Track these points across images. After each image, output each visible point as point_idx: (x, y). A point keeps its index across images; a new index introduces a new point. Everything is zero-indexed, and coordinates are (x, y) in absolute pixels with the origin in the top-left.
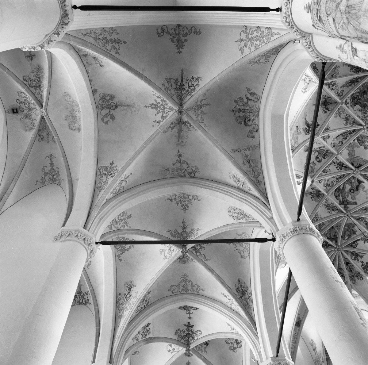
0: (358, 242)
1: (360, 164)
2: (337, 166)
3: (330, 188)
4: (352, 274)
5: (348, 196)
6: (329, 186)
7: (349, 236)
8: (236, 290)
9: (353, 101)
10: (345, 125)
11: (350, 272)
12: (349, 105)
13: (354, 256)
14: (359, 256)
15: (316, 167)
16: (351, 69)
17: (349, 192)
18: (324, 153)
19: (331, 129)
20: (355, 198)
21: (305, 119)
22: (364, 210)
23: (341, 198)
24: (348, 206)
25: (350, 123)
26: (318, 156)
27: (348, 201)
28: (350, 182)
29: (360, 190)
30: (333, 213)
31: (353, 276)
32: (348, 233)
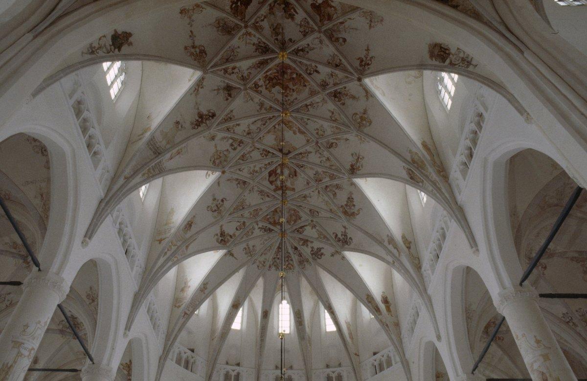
0: (306, 228)
1: (289, 151)
2: (261, 152)
3: (257, 174)
5: (287, 180)
6: (257, 172)
7: (295, 221)
8: (87, 297)
9: (269, 83)
10: (258, 111)
12: (263, 89)
13: (303, 241)
15: (230, 155)
16: (256, 49)
19: (236, 117)
21: (198, 109)
23: (279, 183)
24: (286, 192)
25: (266, 109)
30: (267, 199)
32: (294, 218)
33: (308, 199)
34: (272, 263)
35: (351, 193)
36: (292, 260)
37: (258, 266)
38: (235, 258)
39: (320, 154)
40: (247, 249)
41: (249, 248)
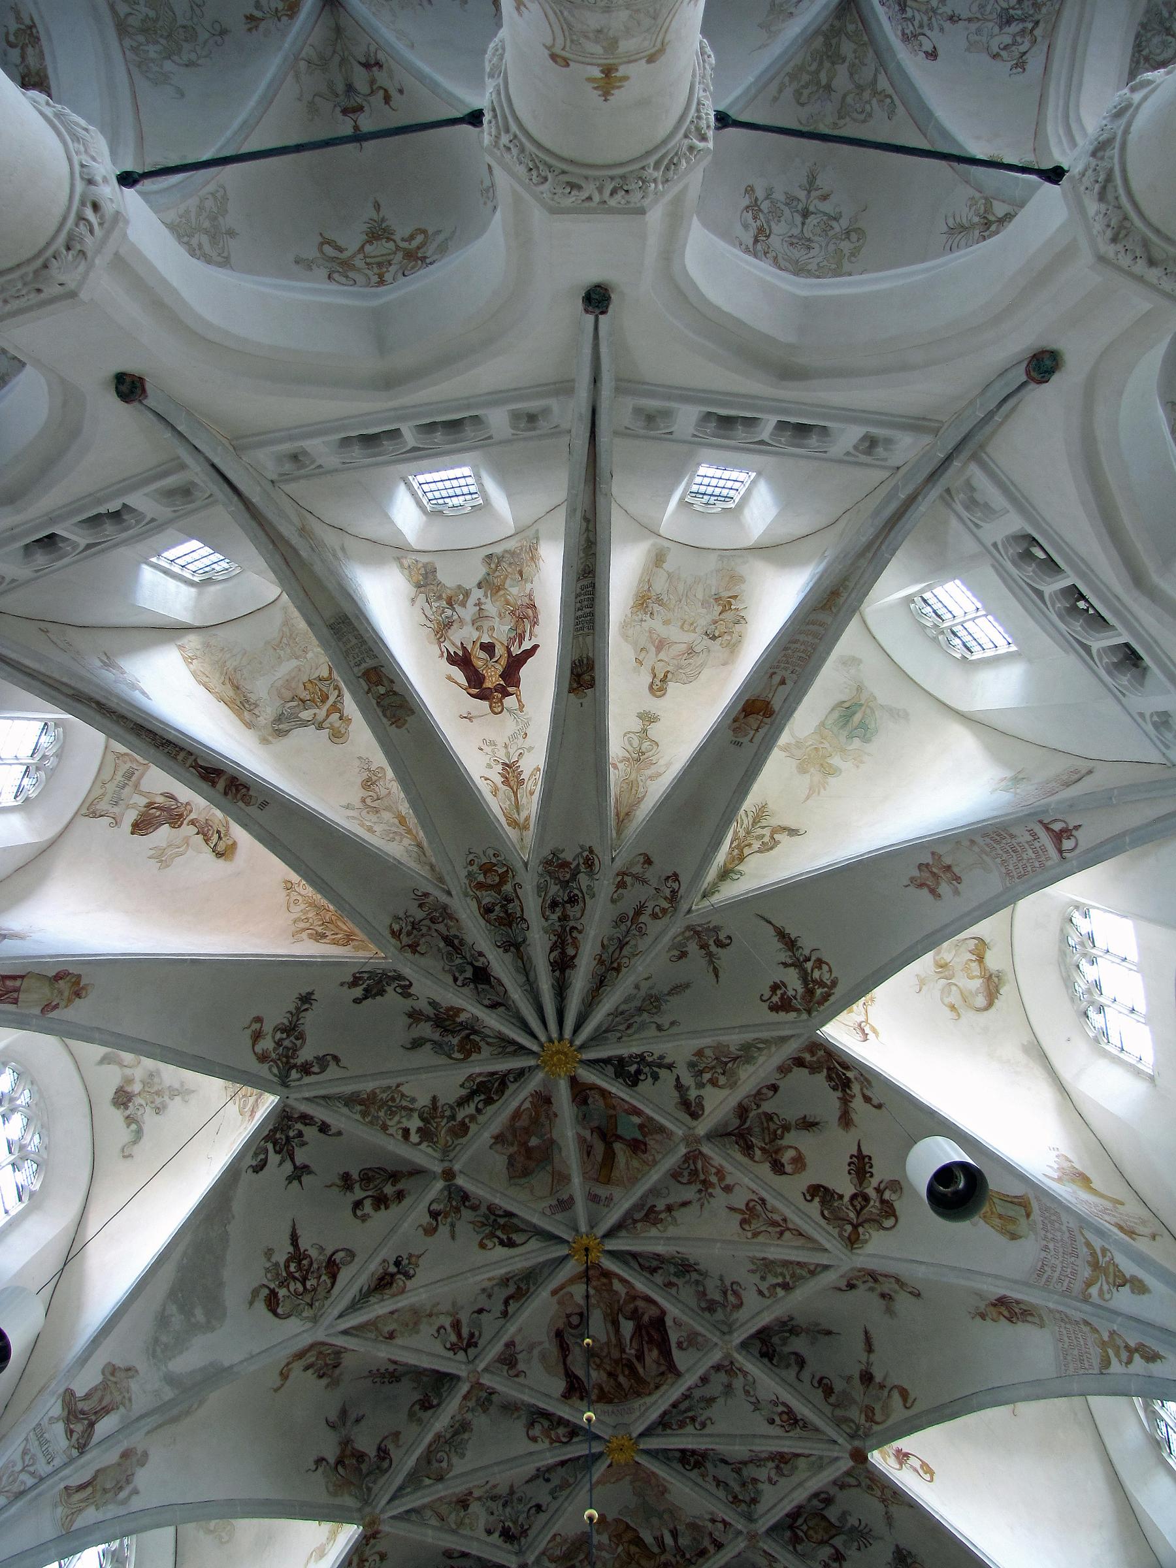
0: (464, 1092)
4: (441, 927)
11: (456, 937)
14: (428, 1019)
18: (800, 1521)
26: (822, 1506)
31: (433, 920)
34: (583, 879)
35: (334, 1383)
36: (487, 910)
37: (648, 861)
38: (770, 923)
39: (494, 1498)
40: (711, 942)
41: (704, 946)
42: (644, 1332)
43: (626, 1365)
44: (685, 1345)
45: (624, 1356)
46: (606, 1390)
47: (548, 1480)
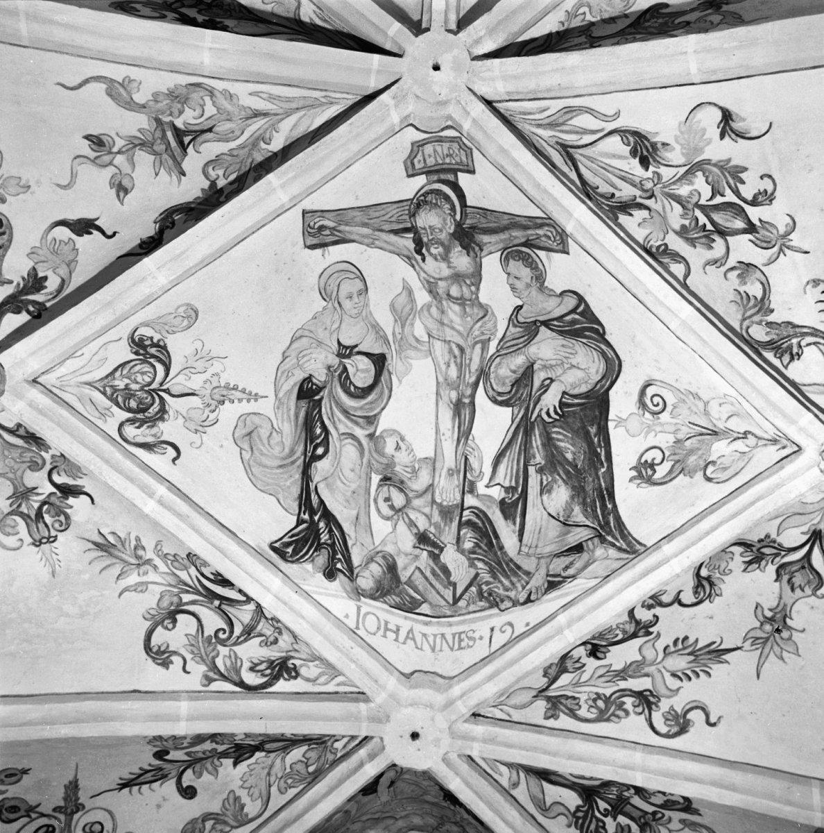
17: (393, 363)
20: (324, 294)
22: (198, 133)
24: (413, 186)
27: (407, 242)
28: (401, 486)
29: (279, 404)
33: (137, 123)
42: (537, 441)
43: (469, 523)
44: (661, 471)
45: (470, 501)
46: (404, 576)
47: (189, 793)
